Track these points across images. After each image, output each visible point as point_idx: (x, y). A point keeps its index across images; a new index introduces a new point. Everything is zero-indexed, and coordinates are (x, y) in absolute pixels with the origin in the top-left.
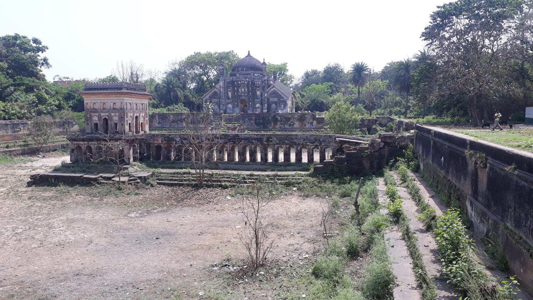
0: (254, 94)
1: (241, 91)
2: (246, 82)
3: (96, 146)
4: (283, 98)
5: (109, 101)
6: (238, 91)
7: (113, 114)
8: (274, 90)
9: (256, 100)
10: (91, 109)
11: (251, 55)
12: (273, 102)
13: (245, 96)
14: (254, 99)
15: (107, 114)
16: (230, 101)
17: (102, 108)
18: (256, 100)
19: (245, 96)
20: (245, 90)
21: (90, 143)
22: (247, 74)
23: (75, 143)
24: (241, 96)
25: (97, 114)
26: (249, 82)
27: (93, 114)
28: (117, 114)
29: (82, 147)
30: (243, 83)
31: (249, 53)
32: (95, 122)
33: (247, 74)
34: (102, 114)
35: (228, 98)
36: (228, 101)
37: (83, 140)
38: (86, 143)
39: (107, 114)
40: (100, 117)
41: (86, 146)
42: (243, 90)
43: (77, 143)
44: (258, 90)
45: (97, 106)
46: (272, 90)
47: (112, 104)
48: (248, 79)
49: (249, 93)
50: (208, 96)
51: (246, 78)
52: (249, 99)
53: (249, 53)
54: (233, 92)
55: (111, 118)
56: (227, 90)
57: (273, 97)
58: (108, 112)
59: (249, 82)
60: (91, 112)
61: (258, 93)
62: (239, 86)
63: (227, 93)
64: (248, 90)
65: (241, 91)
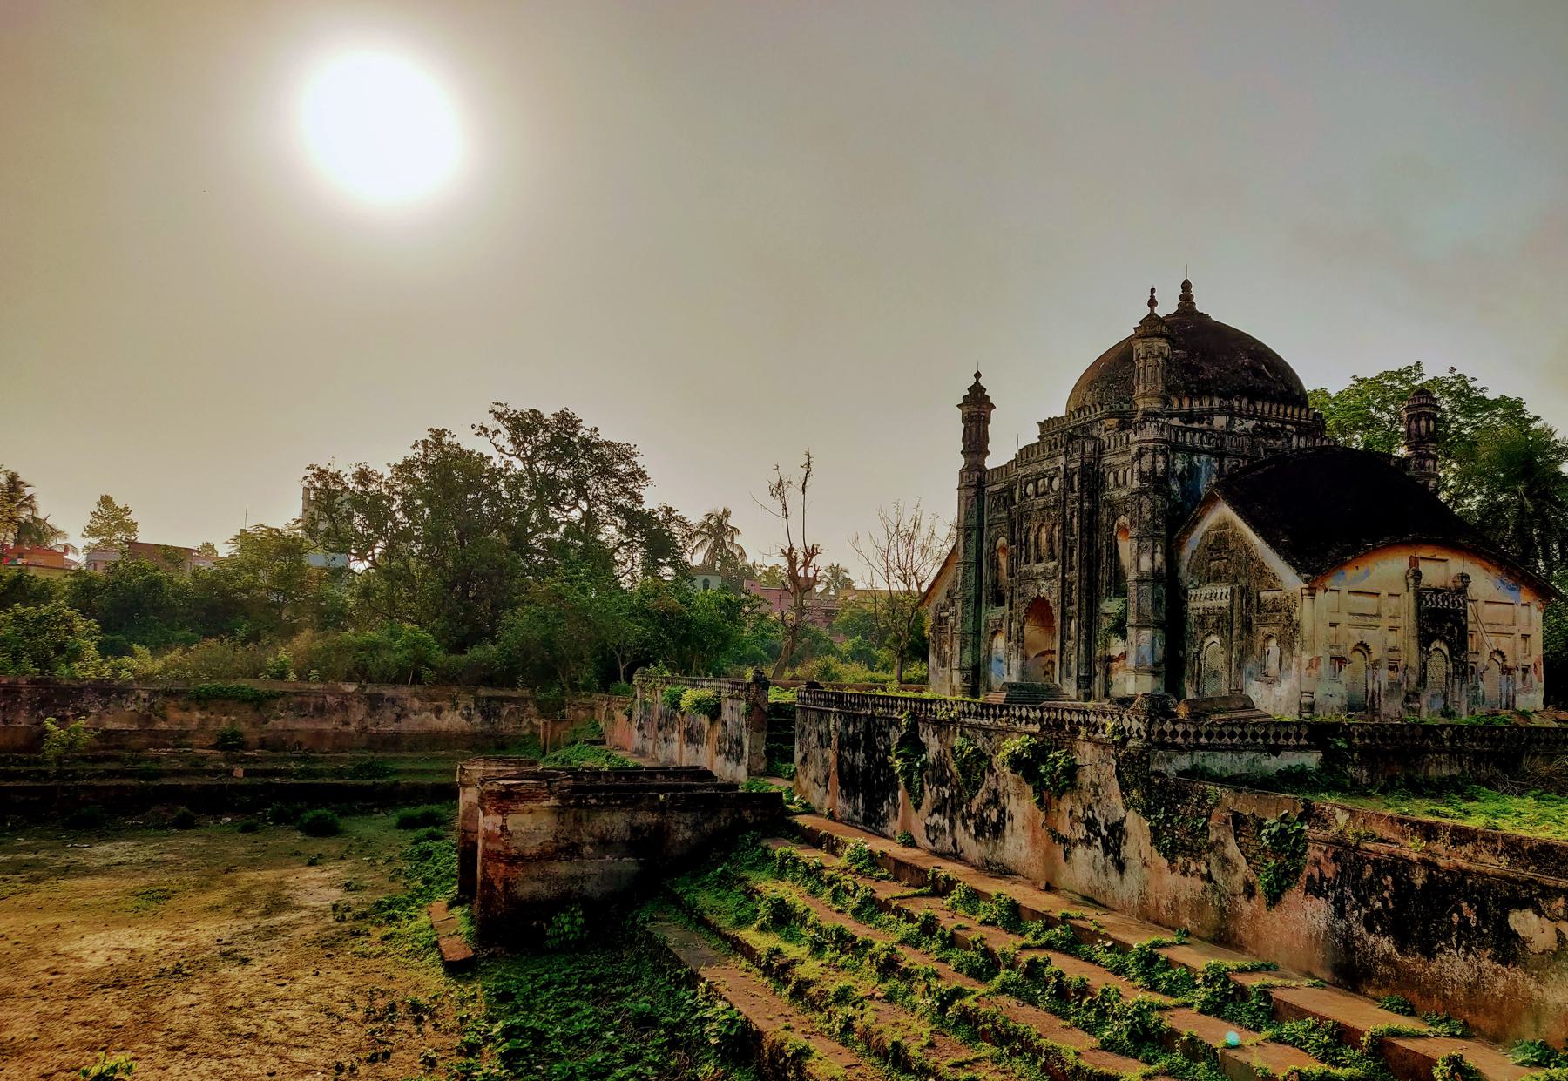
2: (1056, 483)
4: (1272, 582)
11: (1199, 308)
20: (1050, 540)
26: (1068, 477)
42: (1044, 535)
61: (1126, 548)
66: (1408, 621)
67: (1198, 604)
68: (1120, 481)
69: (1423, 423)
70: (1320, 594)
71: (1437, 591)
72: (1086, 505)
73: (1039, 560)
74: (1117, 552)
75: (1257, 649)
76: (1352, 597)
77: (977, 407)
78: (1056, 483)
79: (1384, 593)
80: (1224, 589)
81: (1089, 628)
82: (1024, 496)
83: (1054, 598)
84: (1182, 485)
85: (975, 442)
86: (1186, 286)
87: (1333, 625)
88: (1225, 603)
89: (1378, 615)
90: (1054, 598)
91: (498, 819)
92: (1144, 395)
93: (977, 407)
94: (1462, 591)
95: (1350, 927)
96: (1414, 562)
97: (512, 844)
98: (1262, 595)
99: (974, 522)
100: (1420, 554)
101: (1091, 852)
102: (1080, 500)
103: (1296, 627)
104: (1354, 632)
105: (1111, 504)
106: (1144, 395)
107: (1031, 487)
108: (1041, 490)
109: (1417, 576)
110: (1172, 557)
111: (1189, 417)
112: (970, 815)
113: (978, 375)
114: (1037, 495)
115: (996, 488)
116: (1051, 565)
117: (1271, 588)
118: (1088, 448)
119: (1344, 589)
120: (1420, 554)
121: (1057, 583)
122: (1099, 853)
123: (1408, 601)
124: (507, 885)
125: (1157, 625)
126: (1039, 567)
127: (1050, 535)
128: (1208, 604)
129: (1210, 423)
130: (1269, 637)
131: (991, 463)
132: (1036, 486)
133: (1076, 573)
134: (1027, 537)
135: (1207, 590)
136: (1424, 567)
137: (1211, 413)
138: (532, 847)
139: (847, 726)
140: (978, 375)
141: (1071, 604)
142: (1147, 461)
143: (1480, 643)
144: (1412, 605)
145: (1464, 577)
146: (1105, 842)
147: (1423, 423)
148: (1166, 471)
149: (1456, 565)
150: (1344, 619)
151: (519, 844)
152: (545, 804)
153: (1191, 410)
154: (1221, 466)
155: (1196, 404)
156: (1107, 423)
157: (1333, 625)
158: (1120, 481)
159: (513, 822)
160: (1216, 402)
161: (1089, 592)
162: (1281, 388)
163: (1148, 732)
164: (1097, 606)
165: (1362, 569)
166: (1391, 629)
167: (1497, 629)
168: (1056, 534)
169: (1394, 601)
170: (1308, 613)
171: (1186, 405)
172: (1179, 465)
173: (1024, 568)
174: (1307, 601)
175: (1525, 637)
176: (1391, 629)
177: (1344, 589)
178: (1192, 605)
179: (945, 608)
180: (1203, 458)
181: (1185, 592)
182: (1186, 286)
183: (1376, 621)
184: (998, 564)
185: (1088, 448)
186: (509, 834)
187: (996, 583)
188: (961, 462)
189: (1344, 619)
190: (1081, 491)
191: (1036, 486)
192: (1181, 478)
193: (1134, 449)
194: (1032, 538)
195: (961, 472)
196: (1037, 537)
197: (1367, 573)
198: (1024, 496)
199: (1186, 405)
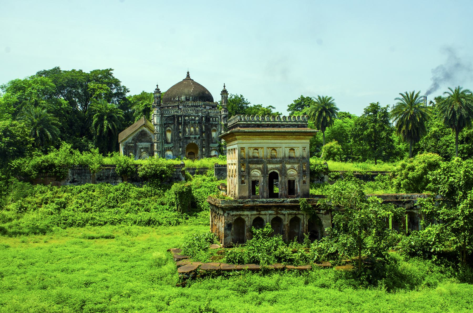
0: (209, 136)
1: (190, 131)
2: (197, 118)
3: (272, 217)
5: (284, 145)
6: (184, 131)
7: (288, 166)
10: (250, 158)
11: (191, 78)
13: (195, 138)
14: (209, 144)
15: (278, 166)
16: (171, 146)
17: (269, 157)
18: (211, 145)
19: (195, 138)
21: (263, 212)
22: (197, 106)
23: (235, 213)
24: (189, 138)
25: (261, 166)
26: (202, 117)
27: (252, 166)
28: (296, 166)
29: (246, 219)
30: (192, 120)
31: (188, 76)
32: (254, 179)
33: (197, 106)
34: (270, 166)
35: (167, 142)
36: (166, 146)
37: (252, 208)
38: (255, 212)
39: (278, 166)
40: (264, 171)
41: (254, 217)
43: (238, 213)
44: (215, 130)
45: (261, 154)
47: (287, 151)
48: (200, 114)
49: (201, 135)
50: (131, 138)
51: (197, 112)
53: (188, 76)
54: (176, 132)
55: (283, 171)
56: (165, 128)
58: (281, 162)
59: (202, 118)
60: (250, 163)
62: (186, 124)
63: (165, 135)
64: (201, 129)
65: (190, 131)
73: (191, 135)
82: (185, 120)
83: (198, 143)
86: (188, 73)
90: (198, 143)
105: (212, 125)
107: (187, 118)
113: (157, 86)
115: (167, 115)
126: (193, 136)
140: (157, 86)
179: (131, 143)
182: (188, 73)
194: (187, 129)
198: (185, 120)
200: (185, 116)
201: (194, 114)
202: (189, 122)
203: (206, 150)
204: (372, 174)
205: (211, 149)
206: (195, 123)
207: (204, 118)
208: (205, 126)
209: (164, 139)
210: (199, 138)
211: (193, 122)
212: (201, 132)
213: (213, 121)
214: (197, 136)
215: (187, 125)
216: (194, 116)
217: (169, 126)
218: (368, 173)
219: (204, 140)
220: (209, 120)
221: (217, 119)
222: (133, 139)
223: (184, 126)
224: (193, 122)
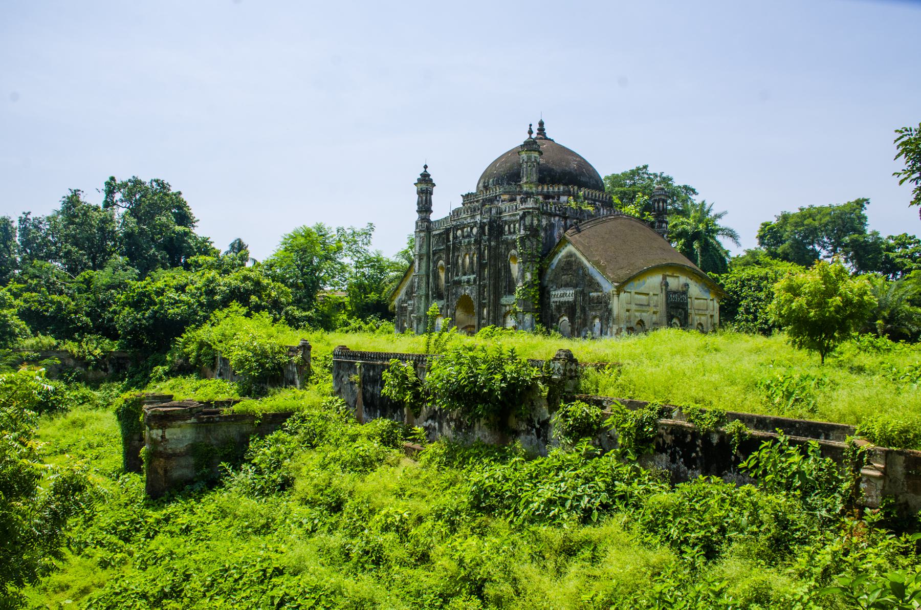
2: (475, 230)
4: (597, 287)
8: (570, 255)
9: (504, 300)
11: (548, 136)
12: (560, 306)
14: (498, 297)
19: (468, 281)
20: (471, 263)
30: (469, 236)
36: (435, 306)
42: (467, 260)
44: (514, 258)
46: (563, 253)
52: (480, 293)
56: (435, 263)
57: (567, 285)
61: (515, 268)
62: (456, 248)
63: (436, 277)
66: (662, 308)
67: (556, 299)
68: (512, 230)
69: (661, 204)
70: (622, 295)
71: (675, 293)
72: (493, 243)
73: (465, 274)
74: (510, 270)
75: (589, 324)
76: (637, 296)
77: (425, 184)
78: (475, 230)
79: (651, 293)
80: (571, 291)
81: (494, 312)
82: (455, 237)
83: (473, 296)
84: (546, 233)
85: (425, 207)
87: (628, 311)
88: (571, 299)
89: (648, 305)
90: (473, 296)
91: (160, 432)
92: (526, 183)
93: (425, 184)
94: (685, 293)
95: (678, 467)
96: (664, 278)
97: (169, 446)
98: (591, 294)
99: (424, 251)
100: (667, 273)
101: (529, 437)
102: (489, 240)
103: (610, 311)
104: (637, 314)
105: (506, 242)
106: (526, 183)
107: (459, 232)
108: (465, 234)
109: (667, 284)
110: (541, 273)
111: (547, 196)
112: (452, 420)
113: (426, 167)
114: (463, 237)
116: (472, 277)
117: (596, 291)
118: (494, 211)
119: (633, 292)
120: (667, 273)
121: (475, 288)
122: (534, 437)
123: (662, 297)
124: (166, 471)
125: (536, 311)
126: (465, 278)
127: (471, 259)
128: (562, 299)
129: (558, 199)
130: (595, 317)
131: (433, 217)
132: (463, 232)
133: (487, 281)
134: (457, 260)
135: (559, 292)
136: (669, 280)
137: (559, 195)
138: (181, 447)
139: (369, 371)
140: (426, 167)
141: (484, 299)
142: (528, 220)
143: (693, 320)
144: (664, 299)
145: (687, 285)
146: (538, 431)
147: (661, 204)
148: (538, 225)
149: (683, 279)
150: (633, 307)
151: (173, 446)
152: (189, 421)
153: (548, 192)
154: (566, 224)
155: (551, 189)
156: (503, 197)
157: (628, 311)
158: (512, 230)
159: (169, 433)
160: (562, 188)
161: (494, 293)
162: (593, 182)
163: (565, 370)
164: (499, 299)
165: (641, 281)
166: (654, 313)
167: (700, 312)
168: (475, 259)
169: (656, 298)
170: (617, 305)
171: (545, 190)
172: (544, 222)
173: (456, 278)
174: (616, 298)
175: (712, 316)
176: (654, 313)
177: (633, 292)
178: (552, 300)
179: (404, 301)
180: (557, 218)
181: (549, 292)
183: (645, 308)
184: (439, 276)
185: (494, 211)
186: (167, 440)
187: (437, 286)
188: (416, 216)
189: (633, 307)
190: (490, 234)
191: (463, 232)
192: (545, 230)
193: (521, 213)
194: (460, 261)
195: (417, 223)
196: (463, 261)
197: (644, 283)
198: (455, 237)
199: (545, 190)
200: (456, 228)
201: (469, 220)
202: (460, 242)
203: (488, 313)
204: (750, 431)
205: (503, 310)
206: (469, 243)
207: (487, 228)
208: (490, 247)
209: (432, 290)
210: (475, 279)
211: (466, 240)
212: (482, 266)
213: (510, 233)
214: (472, 277)
215: (459, 249)
216: (468, 225)
217: (440, 258)
218: (729, 428)
219: (485, 286)
220: (501, 232)
221: (517, 225)
222: (407, 294)
223: (453, 253)
224: (466, 240)
